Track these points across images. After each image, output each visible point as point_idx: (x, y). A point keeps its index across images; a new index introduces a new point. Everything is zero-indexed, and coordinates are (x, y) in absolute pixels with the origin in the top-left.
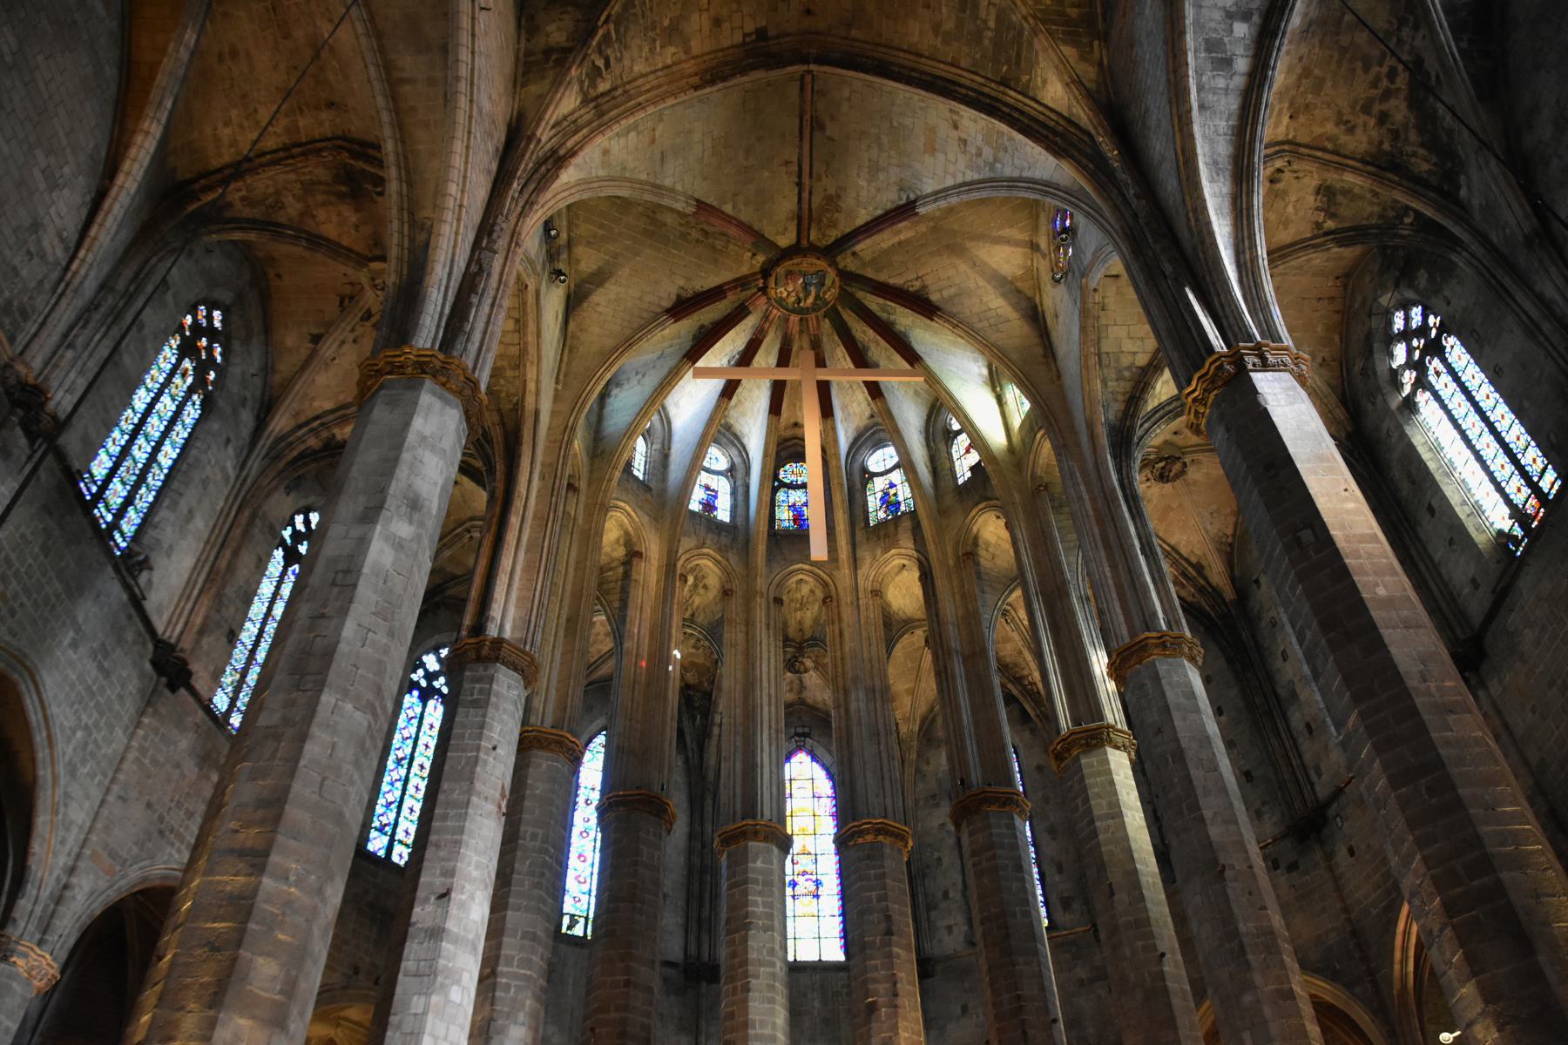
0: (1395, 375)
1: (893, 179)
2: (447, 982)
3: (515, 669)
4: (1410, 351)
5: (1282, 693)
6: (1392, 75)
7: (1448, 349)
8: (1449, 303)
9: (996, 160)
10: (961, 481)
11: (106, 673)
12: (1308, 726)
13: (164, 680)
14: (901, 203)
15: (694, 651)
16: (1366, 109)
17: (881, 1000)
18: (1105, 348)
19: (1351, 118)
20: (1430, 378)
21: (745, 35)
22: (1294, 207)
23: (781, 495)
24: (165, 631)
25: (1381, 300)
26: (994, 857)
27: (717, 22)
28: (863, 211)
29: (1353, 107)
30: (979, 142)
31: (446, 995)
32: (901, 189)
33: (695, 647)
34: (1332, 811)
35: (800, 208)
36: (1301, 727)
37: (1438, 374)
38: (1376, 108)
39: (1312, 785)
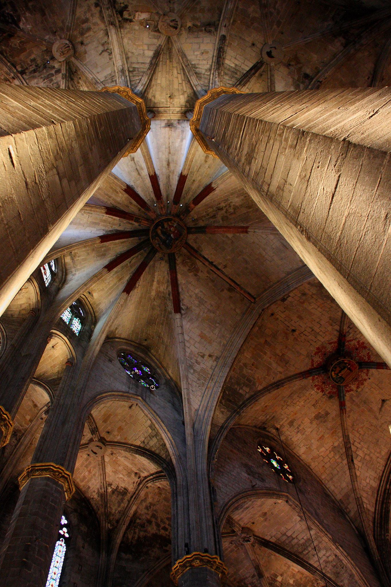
1: (194, 308)
6: (165, 529)
9: (194, 370)
14: (181, 304)
15: (32, 57)
16: (153, 516)
19: (151, 509)
21: (289, 296)
22: (121, 478)
27: (304, 294)
28: (183, 282)
29: (155, 511)
30: (202, 366)
32: (187, 308)
33: (34, 60)
35: (200, 255)
38: (153, 520)
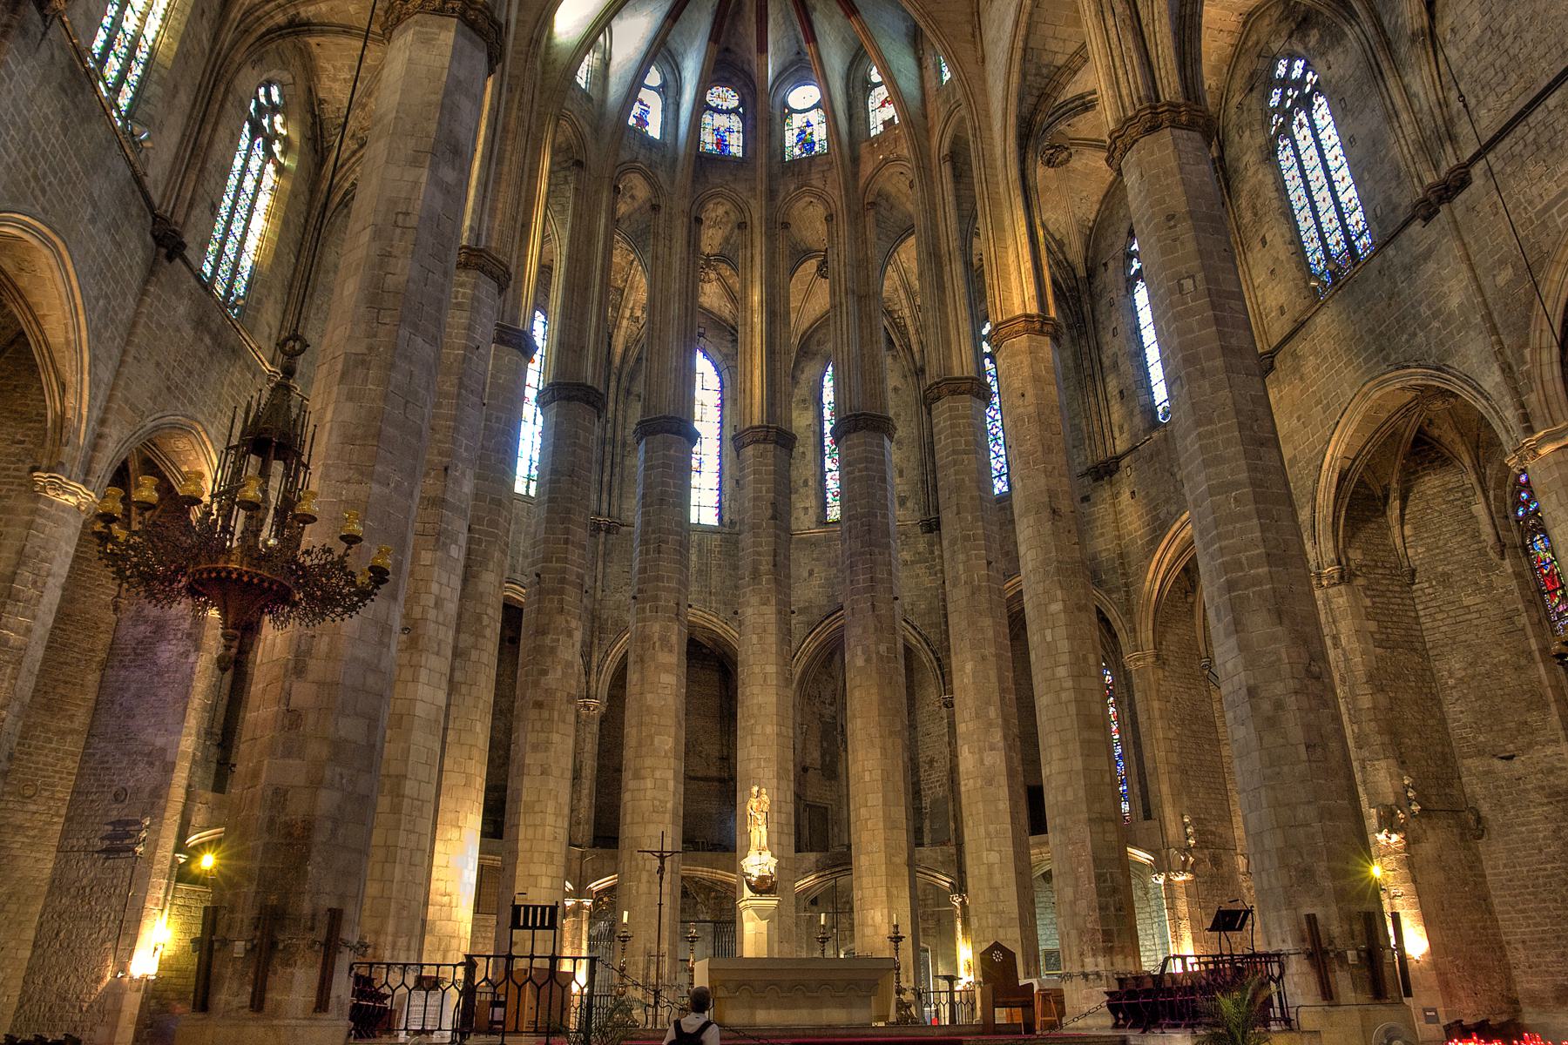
0: (1267, 114)
2: (448, 541)
3: (493, 278)
4: (1284, 98)
5: (1106, 362)
7: (1316, 107)
8: (1329, 68)
10: (873, 133)
11: (119, 245)
12: (1121, 392)
13: (164, 251)
17: (764, 568)
18: (1031, 45)
20: (1294, 127)
23: (707, 118)
24: (161, 205)
25: (1272, 45)
26: (867, 469)
31: (448, 552)
34: (1124, 463)
36: (1116, 392)
37: (1301, 125)
39: (1114, 439)
